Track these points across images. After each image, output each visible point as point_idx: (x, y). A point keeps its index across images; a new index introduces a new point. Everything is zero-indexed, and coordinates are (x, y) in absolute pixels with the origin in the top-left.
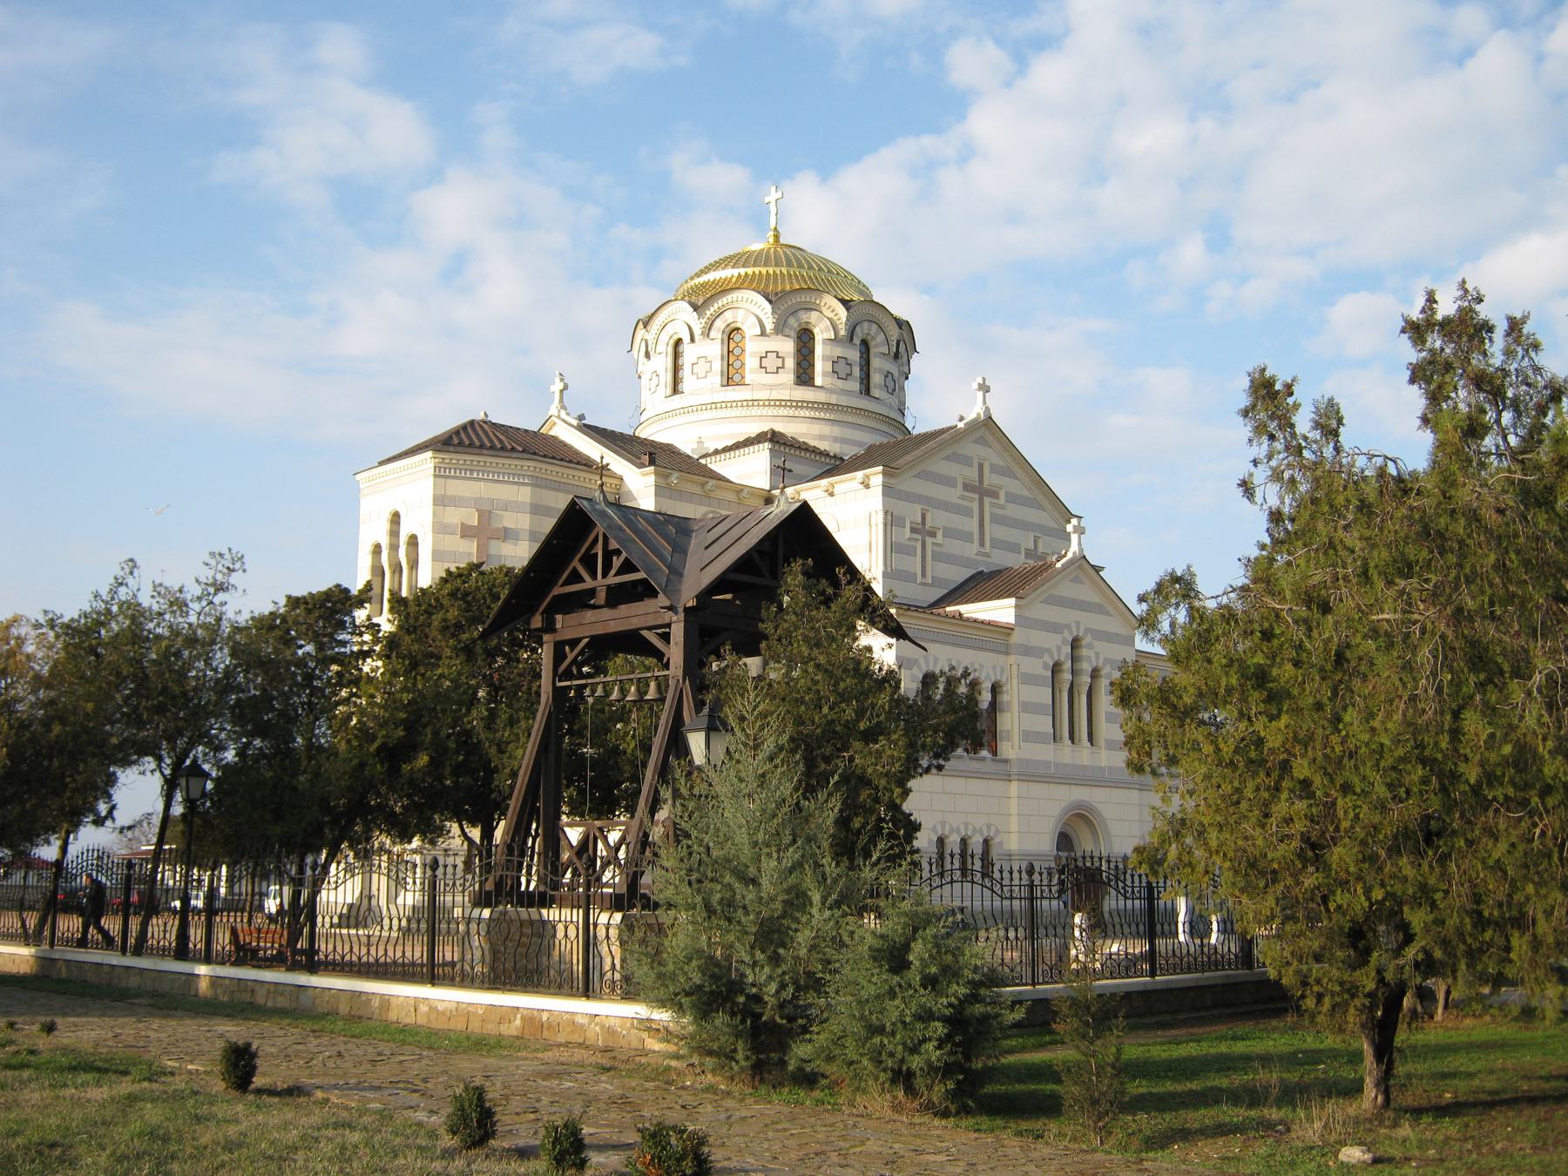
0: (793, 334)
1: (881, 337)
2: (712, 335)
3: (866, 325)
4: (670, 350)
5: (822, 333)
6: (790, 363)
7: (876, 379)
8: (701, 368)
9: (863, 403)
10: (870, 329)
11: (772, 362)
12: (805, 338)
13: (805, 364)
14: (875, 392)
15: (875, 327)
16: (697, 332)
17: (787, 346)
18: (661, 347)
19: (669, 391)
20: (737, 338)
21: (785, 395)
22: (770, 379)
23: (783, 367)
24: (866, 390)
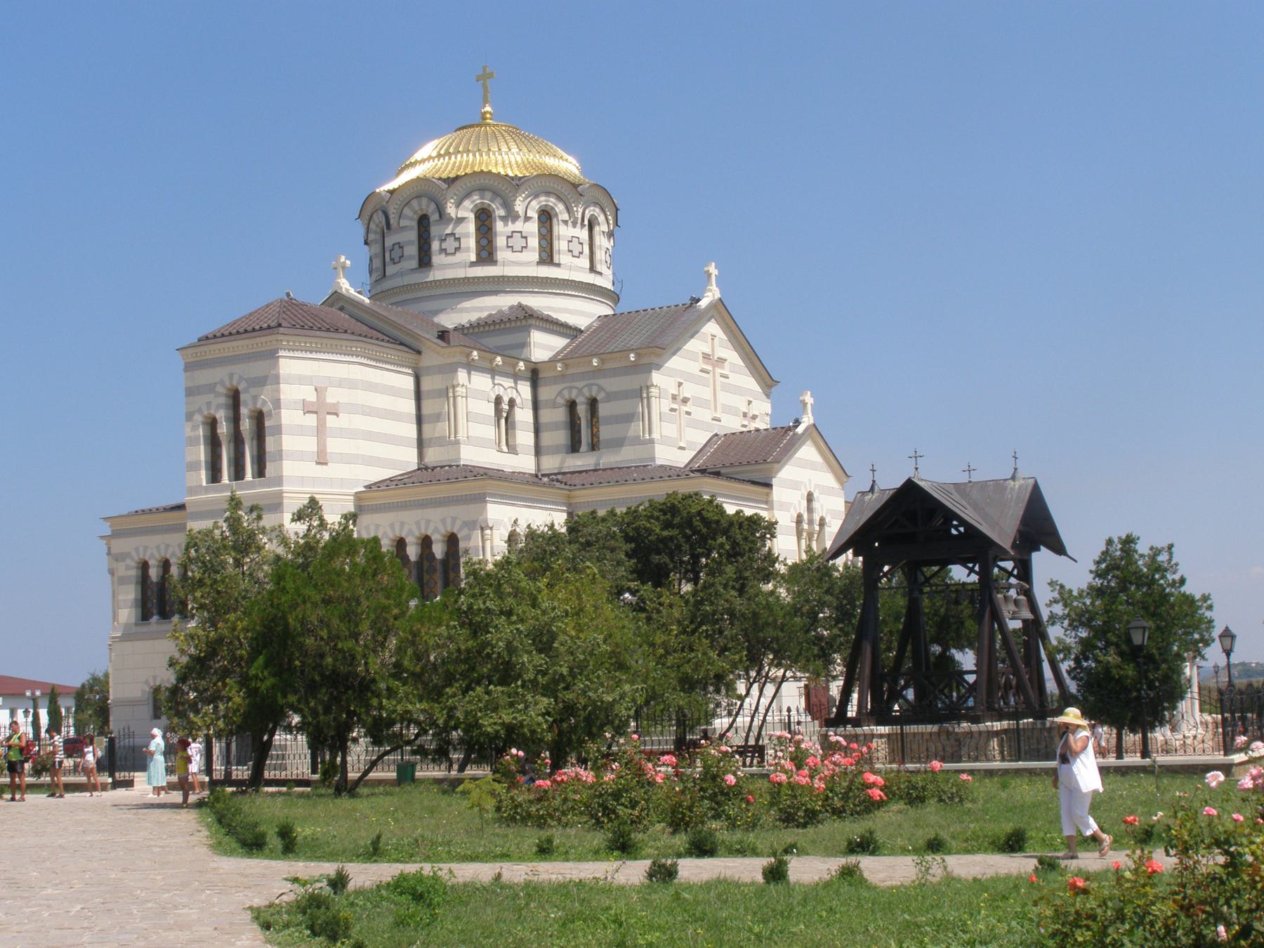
0: (472, 216)
1: (560, 207)
2: (403, 223)
4: (378, 237)
6: (471, 243)
7: (561, 245)
8: (396, 255)
11: (450, 244)
12: (484, 217)
13: (484, 242)
14: (556, 260)
16: (392, 221)
18: (371, 237)
21: (461, 273)
22: (451, 259)
24: (547, 257)
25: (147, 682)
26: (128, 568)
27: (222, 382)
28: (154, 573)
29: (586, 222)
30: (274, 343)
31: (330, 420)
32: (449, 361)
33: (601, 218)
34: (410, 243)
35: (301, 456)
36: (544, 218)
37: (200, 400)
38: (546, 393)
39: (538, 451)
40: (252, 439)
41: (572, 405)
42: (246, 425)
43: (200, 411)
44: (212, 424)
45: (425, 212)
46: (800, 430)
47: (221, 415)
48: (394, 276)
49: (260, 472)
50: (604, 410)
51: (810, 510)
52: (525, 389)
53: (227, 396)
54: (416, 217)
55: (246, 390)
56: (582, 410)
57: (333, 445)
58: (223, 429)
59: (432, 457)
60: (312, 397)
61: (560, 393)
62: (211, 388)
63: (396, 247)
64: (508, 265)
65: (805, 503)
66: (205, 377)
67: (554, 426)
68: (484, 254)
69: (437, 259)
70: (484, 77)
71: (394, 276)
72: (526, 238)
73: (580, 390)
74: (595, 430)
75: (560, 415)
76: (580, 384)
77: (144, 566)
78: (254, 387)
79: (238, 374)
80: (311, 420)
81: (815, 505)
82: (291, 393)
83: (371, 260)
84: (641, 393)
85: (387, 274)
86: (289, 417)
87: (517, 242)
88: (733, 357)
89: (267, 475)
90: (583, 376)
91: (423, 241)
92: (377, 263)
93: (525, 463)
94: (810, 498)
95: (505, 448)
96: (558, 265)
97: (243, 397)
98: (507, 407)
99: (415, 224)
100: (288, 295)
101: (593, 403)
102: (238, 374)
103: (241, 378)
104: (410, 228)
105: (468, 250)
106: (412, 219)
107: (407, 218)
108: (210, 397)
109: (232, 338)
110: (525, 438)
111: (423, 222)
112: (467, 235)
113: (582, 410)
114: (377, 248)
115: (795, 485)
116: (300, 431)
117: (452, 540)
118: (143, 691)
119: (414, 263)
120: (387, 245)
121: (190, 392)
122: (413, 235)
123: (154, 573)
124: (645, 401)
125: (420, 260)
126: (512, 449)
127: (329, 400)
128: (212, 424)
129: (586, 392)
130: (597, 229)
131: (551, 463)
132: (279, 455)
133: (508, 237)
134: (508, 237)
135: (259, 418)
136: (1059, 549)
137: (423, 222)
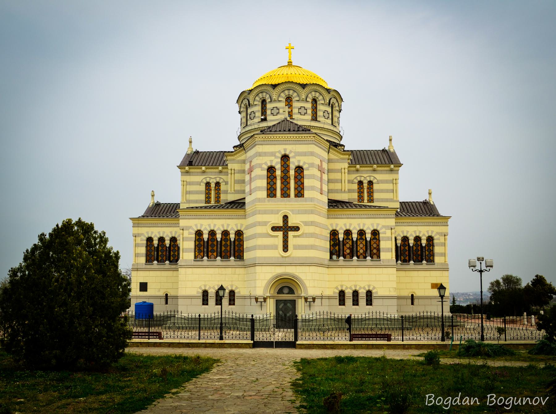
1: (337, 104)
3: (333, 99)
4: (260, 104)
5: (320, 101)
6: (309, 112)
7: (335, 119)
8: (275, 111)
9: (332, 128)
10: (334, 101)
11: (303, 111)
14: (336, 124)
15: (335, 100)
17: (309, 105)
19: (260, 120)
23: (306, 113)
25: (200, 288)
26: (190, 234)
27: (279, 152)
28: (206, 237)
30: (312, 137)
41: (360, 183)
42: (292, 173)
43: (266, 163)
44: (271, 169)
45: (290, 96)
47: (278, 167)
49: (300, 194)
50: (375, 187)
54: (285, 98)
55: (294, 157)
56: (365, 185)
58: (278, 173)
60: (320, 165)
61: (356, 178)
62: (273, 154)
68: (314, 118)
72: (329, 114)
75: (355, 187)
76: (365, 175)
77: (199, 233)
79: (289, 149)
87: (326, 114)
89: (305, 197)
92: (259, 114)
97: (291, 160)
99: (285, 100)
101: (370, 183)
103: (291, 152)
107: (282, 97)
108: (272, 158)
109: (295, 132)
111: (289, 100)
112: (309, 108)
113: (365, 185)
114: (257, 109)
117: (375, 233)
118: (198, 292)
123: (206, 237)
124: (395, 185)
127: (323, 167)
129: (368, 179)
135: (299, 169)
137: (289, 100)
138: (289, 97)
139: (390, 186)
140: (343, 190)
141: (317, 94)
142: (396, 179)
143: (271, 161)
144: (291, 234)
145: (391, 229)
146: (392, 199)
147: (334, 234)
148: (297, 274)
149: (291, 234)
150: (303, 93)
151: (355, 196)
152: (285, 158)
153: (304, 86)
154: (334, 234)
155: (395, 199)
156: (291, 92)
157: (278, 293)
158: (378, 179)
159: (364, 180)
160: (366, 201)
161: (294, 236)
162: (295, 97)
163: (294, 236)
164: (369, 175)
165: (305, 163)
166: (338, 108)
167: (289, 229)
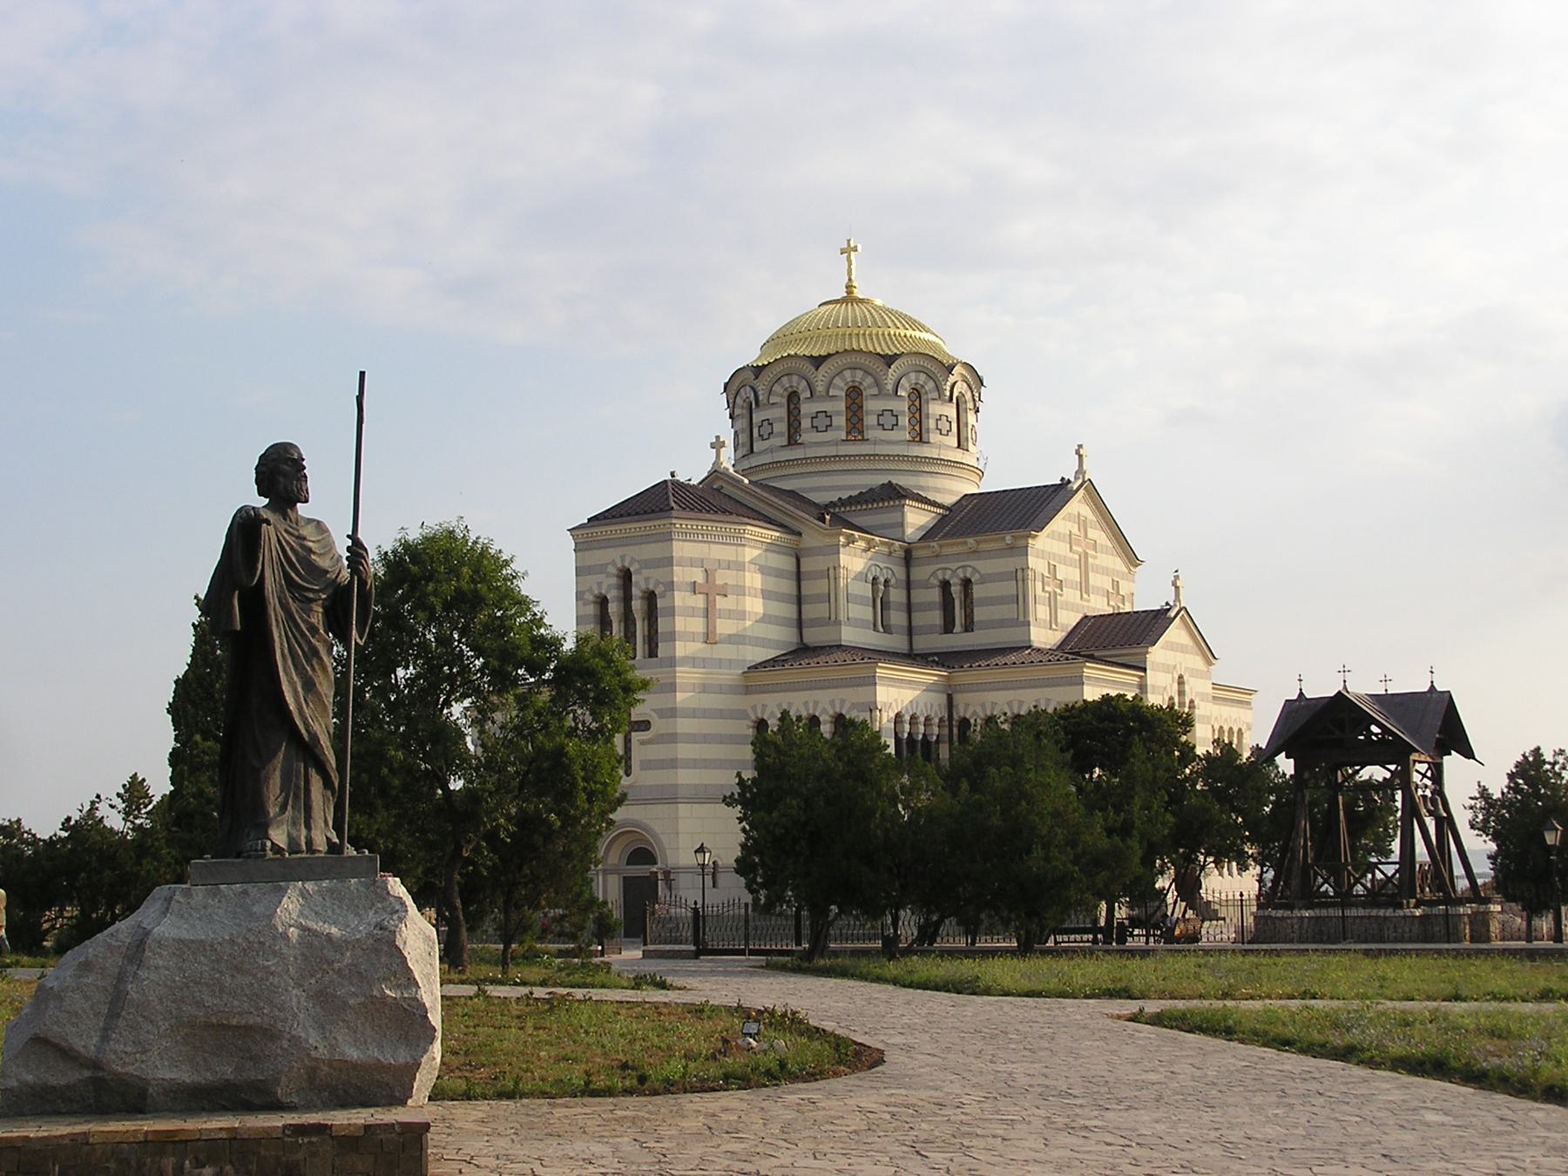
0: (844, 394)
1: (931, 385)
3: (913, 375)
6: (840, 421)
8: (766, 430)
11: (821, 422)
15: (923, 377)
16: (761, 398)
18: (737, 411)
20: (795, 401)
21: (832, 451)
29: (955, 400)
31: (721, 602)
32: (827, 541)
33: (968, 396)
34: (781, 420)
35: (692, 637)
36: (913, 397)
37: (592, 580)
38: (919, 573)
39: (910, 631)
40: (644, 619)
41: (945, 586)
42: (637, 605)
43: (591, 590)
44: (603, 602)
46: (1172, 614)
47: (612, 595)
48: (760, 453)
50: (978, 591)
51: (1181, 693)
52: (900, 572)
53: (618, 576)
54: (786, 394)
55: (639, 572)
56: (956, 590)
57: (724, 627)
58: (614, 609)
59: (813, 636)
62: (601, 569)
63: (765, 423)
64: (880, 444)
65: (1176, 686)
66: (597, 557)
67: (928, 607)
69: (806, 437)
70: (848, 250)
71: (760, 453)
73: (954, 572)
74: (969, 611)
75: (935, 595)
76: (954, 566)
78: (647, 567)
79: (631, 556)
80: (699, 601)
81: (1187, 688)
82: (680, 574)
83: (736, 432)
84: (1020, 576)
85: (755, 450)
86: (681, 599)
87: (888, 420)
88: (1099, 535)
90: (958, 556)
91: (792, 418)
92: (744, 438)
93: (898, 642)
94: (1181, 679)
95: (881, 630)
96: (928, 442)
98: (883, 588)
99: (784, 401)
100: (673, 475)
101: (967, 583)
102: (631, 556)
103: (633, 560)
104: (781, 405)
105: (839, 428)
106: (782, 396)
108: (600, 578)
110: (897, 618)
112: (838, 413)
114: (742, 423)
115: (1168, 669)
116: (692, 612)
119: (785, 443)
120: (754, 421)
121: (579, 572)
122: (782, 412)
124: (1020, 583)
125: (789, 437)
126: (887, 629)
128: (603, 602)
130: (962, 407)
131: (922, 643)
132: (672, 636)
133: (879, 415)
134: (879, 415)
135: (651, 597)
136: (1468, 753)
137: (793, 397)
138: (795, 392)
139: (1008, 588)
140: (833, 618)
141: (859, 374)
142: (1023, 570)
143: (599, 584)
144: (636, 736)
145: (871, 710)
146: (1012, 620)
147: (761, 725)
148: (648, 822)
149: (636, 736)
150: (820, 377)
151: (936, 617)
152: (626, 576)
153: (818, 361)
154: (761, 725)
155: (1021, 618)
156: (795, 378)
157: (628, 864)
158: (982, 572)
159: (952, 577)
160: (958, 628)
161: (643, 743)
162: (803, 391)
163: (643, 743)
164: (963, 564)
165: (657, 583)
166: (935, 395)
167: (636, 728)
